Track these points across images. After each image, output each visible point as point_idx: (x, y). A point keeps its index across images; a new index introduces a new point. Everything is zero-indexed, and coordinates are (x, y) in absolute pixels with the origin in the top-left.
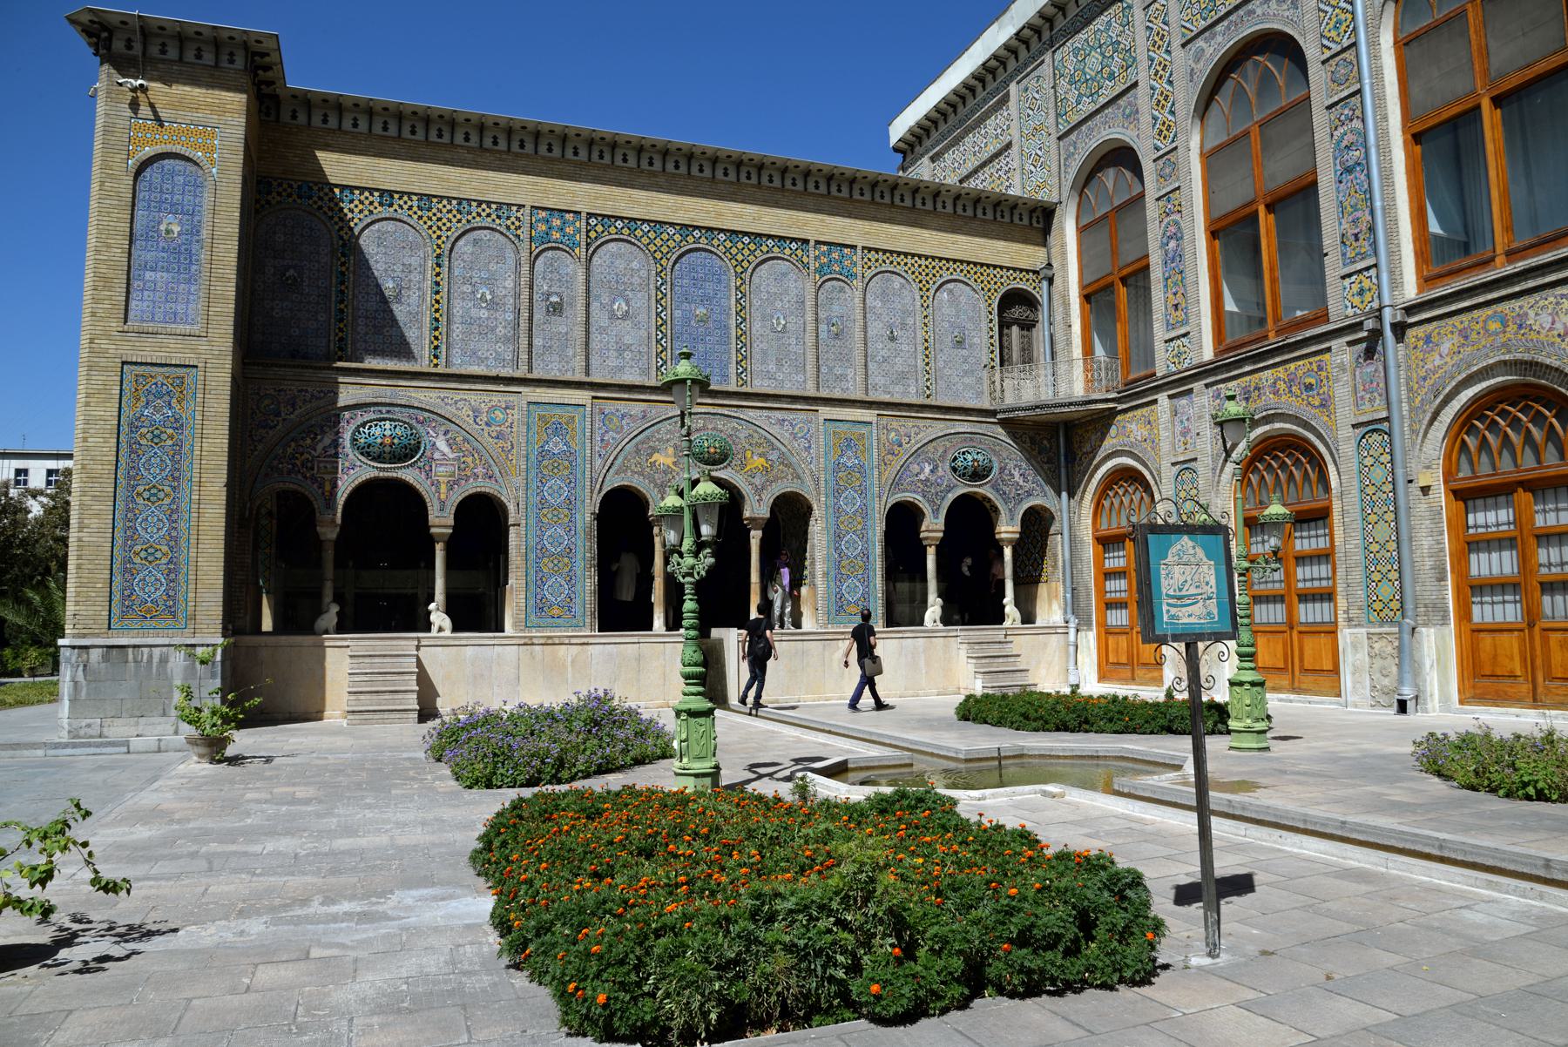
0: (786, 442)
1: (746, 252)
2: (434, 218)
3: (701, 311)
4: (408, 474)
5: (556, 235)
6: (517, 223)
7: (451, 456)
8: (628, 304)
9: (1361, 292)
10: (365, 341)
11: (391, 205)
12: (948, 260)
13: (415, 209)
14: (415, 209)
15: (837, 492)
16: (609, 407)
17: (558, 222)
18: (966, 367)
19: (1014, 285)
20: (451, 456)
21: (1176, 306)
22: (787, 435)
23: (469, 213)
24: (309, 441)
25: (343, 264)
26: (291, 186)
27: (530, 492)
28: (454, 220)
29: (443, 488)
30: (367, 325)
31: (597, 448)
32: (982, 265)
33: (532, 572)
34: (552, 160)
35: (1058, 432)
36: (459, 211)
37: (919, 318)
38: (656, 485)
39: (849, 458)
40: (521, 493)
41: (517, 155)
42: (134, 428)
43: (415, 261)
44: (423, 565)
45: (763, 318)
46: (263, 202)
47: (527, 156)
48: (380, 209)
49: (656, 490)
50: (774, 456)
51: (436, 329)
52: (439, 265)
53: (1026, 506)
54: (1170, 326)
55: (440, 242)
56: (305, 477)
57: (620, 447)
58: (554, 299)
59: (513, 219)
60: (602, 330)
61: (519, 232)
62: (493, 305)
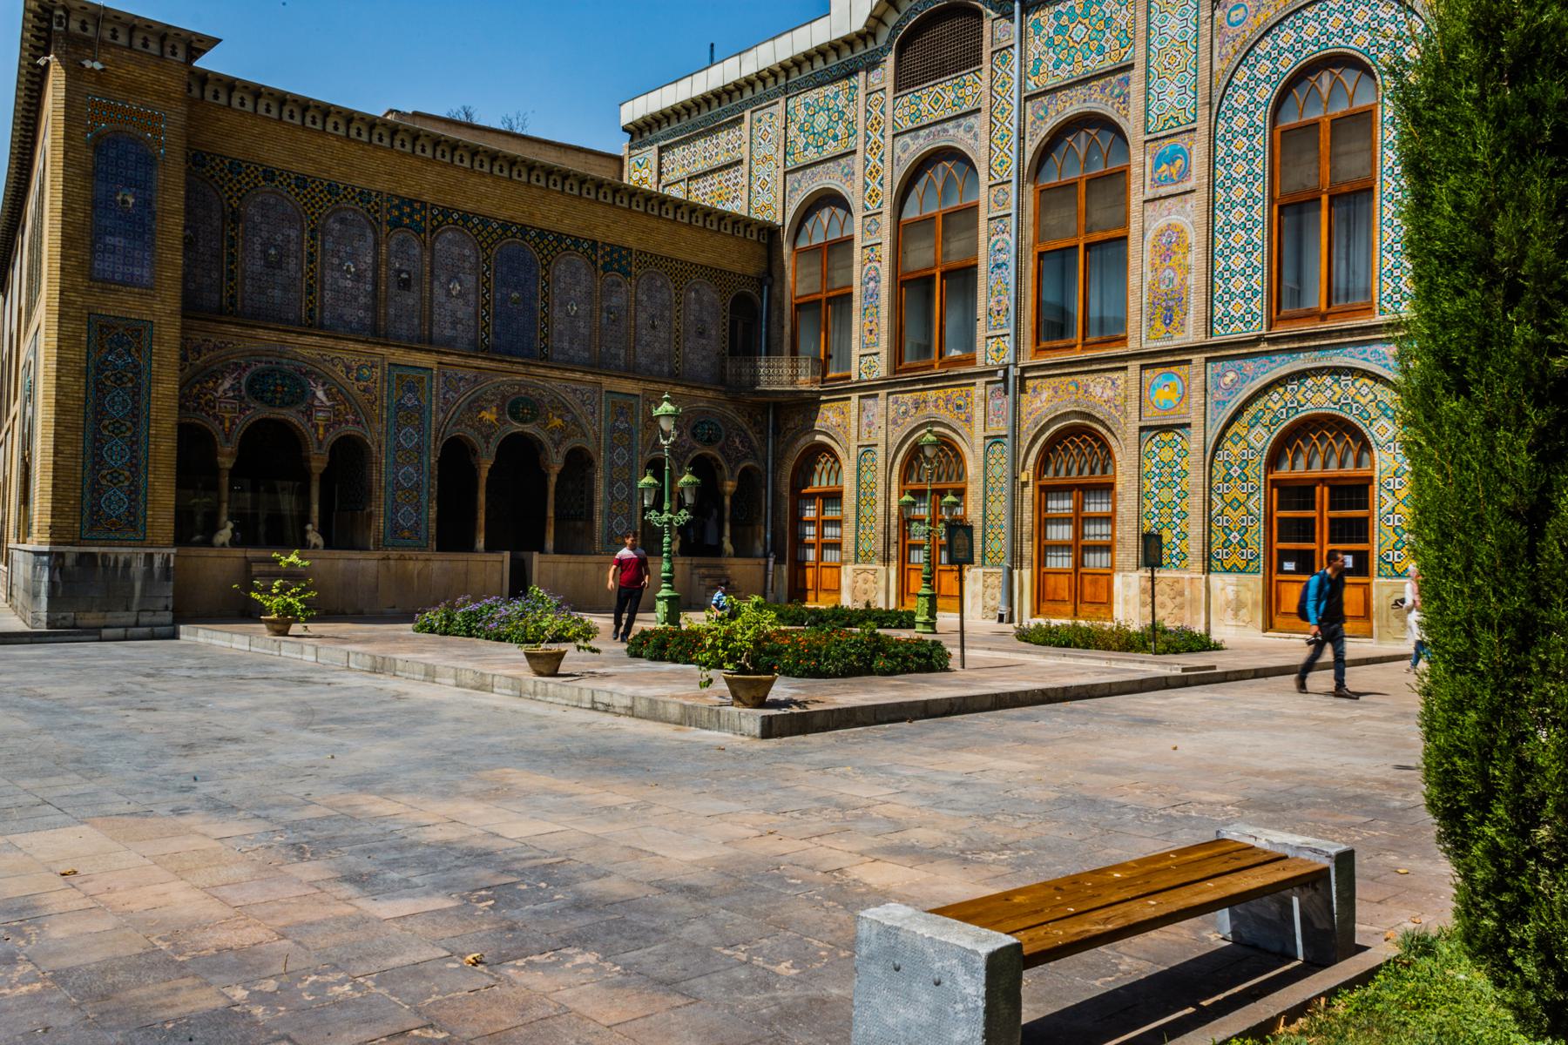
3: (515, 295)
7: (328, 404)
9: (998, 350)
11: (273, 181)
15: (612, 448)
18: (704, 353)
21: (871, 331)
23: (338, 195)
25: (232, 230)
29: (321, 431)
30: (253, 286)
34: (404, 154)
38: (483, 437)
41: (376, 147)
45: (561, 304)
47: (384, 148)
52: (313, 238)
53: (742, 465)
54: (864, 345)
56: (208, 414)
58: (404, 276)
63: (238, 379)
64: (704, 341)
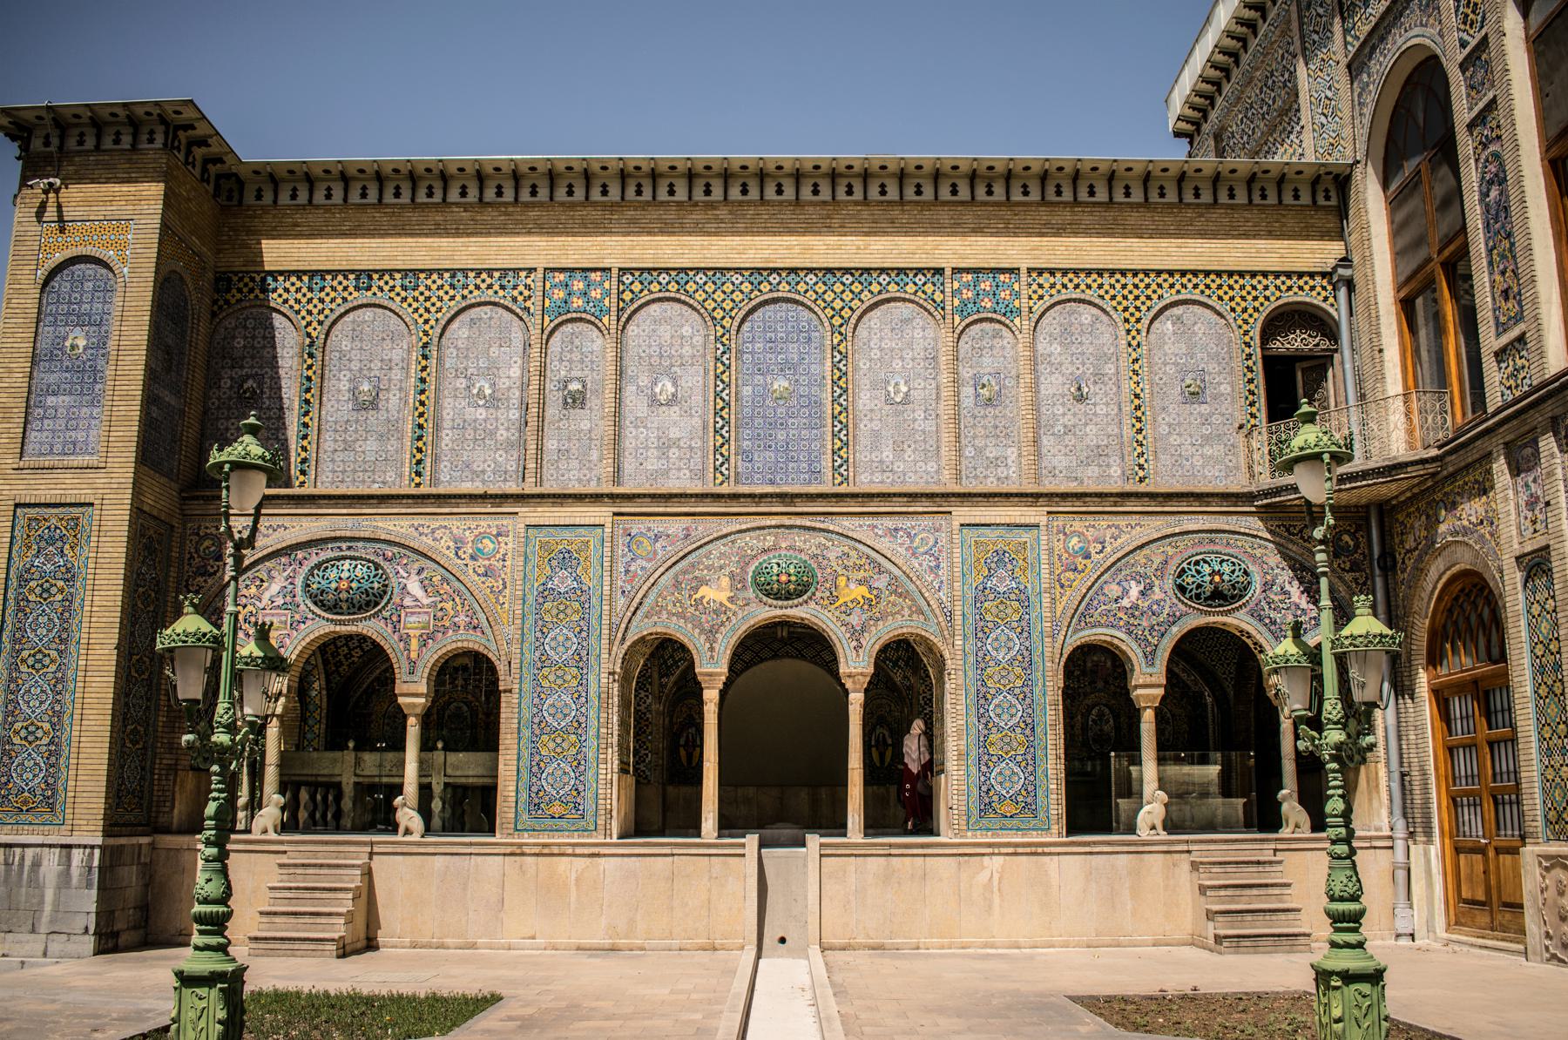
0: (900, 562)
1: (847, 296)
2: (421, 298)
3: (780, 384)
4: (371, 627)
5: (577, 302)
6: (526, 293)
7: (426, 601)
8: (675, 384)
10: (333, 461)
11: (369, 288)
12: (1171, 273)
13: (398, 289)
14: (398, 289)
16: (637, 525)
17: (581, 285)
18: (1206, 430)
19: (1289, 298)
20: (426, 601)
22: (902, 550)
23: (465, 286)
24: (253, 590)
26: (253, 280)
27: (526, 645)
28: (446, 298)
29: (414, 644)
31: (620, 583)
32: (1231, 274)
33: (526, 754)
35: (1367, 520)
36: (452, 286)
37: (1125, 363)
38: (702, 631)
39: (1001, 580)
40: (515, 648)
41: (527, 205)
42: (23, 581)
43: (397, 355)
44: (351, 744)
45: (874, 387)
46: (221, 302)
47: (541, 204)
48: (356, 294)
49: (703, 637)
50: (881, 582)
51: (420, 438)
52: (425, 357)
54: (1501, 328)
55: (427, 327)
57: (652, 580)
59: (521, 288)
60: (640, 422)
61: (528, 304)
62: (493, 402)
63: (291, 579)
64: (1204, 409)
